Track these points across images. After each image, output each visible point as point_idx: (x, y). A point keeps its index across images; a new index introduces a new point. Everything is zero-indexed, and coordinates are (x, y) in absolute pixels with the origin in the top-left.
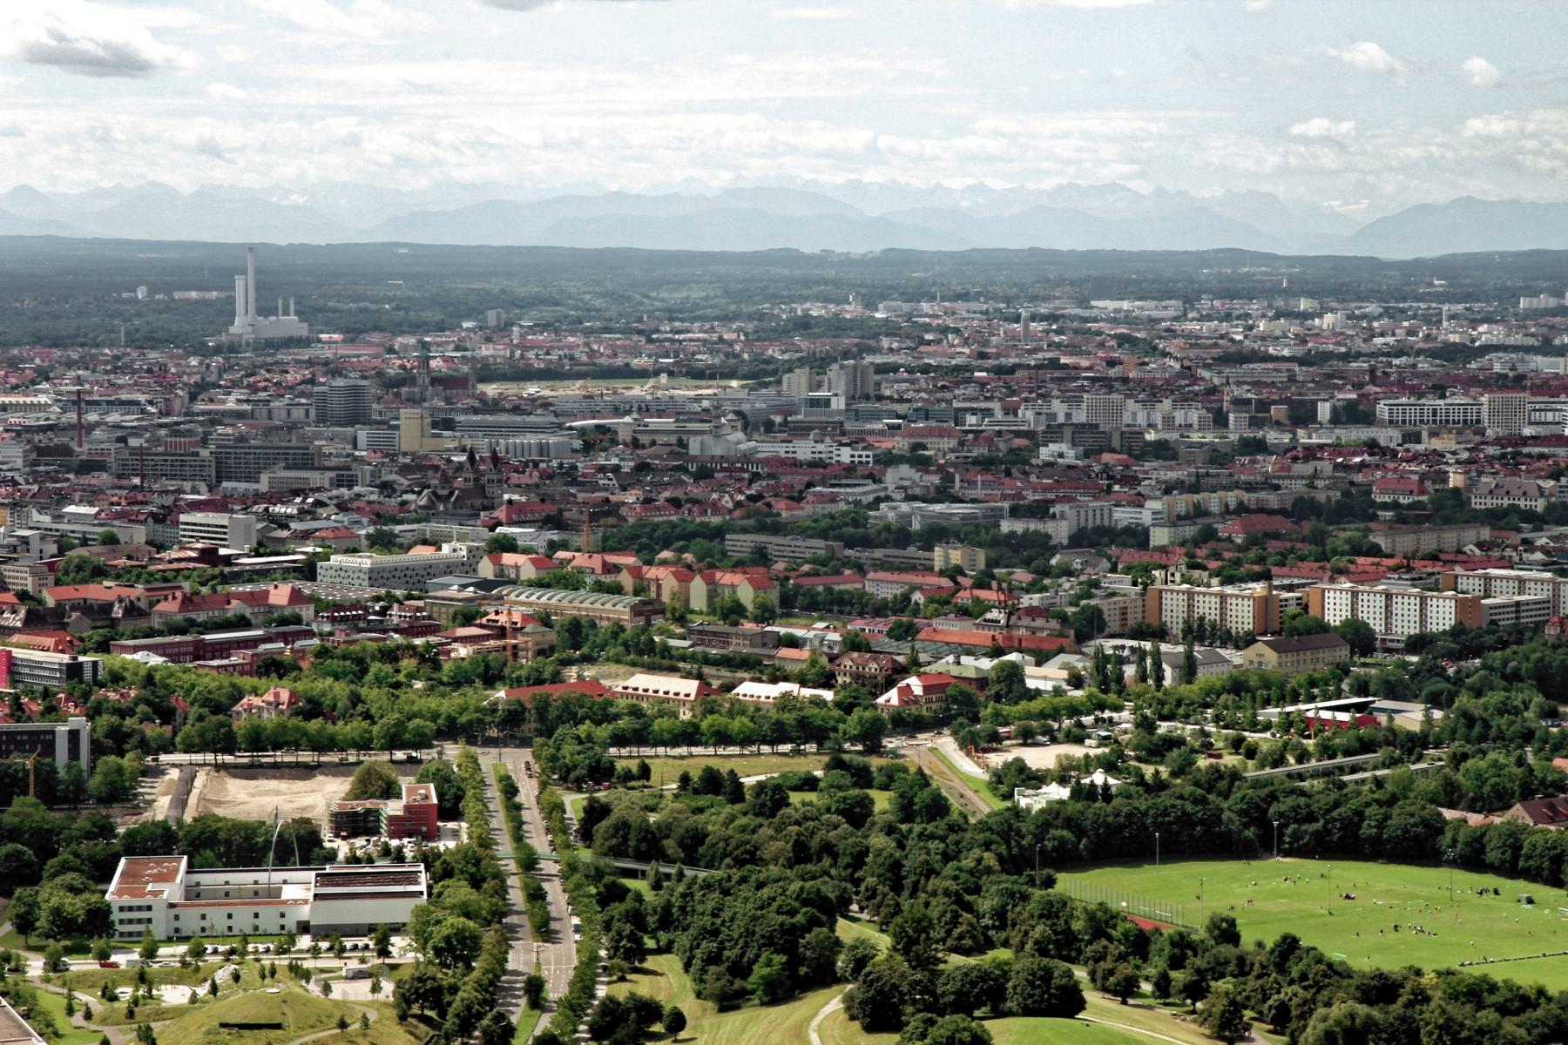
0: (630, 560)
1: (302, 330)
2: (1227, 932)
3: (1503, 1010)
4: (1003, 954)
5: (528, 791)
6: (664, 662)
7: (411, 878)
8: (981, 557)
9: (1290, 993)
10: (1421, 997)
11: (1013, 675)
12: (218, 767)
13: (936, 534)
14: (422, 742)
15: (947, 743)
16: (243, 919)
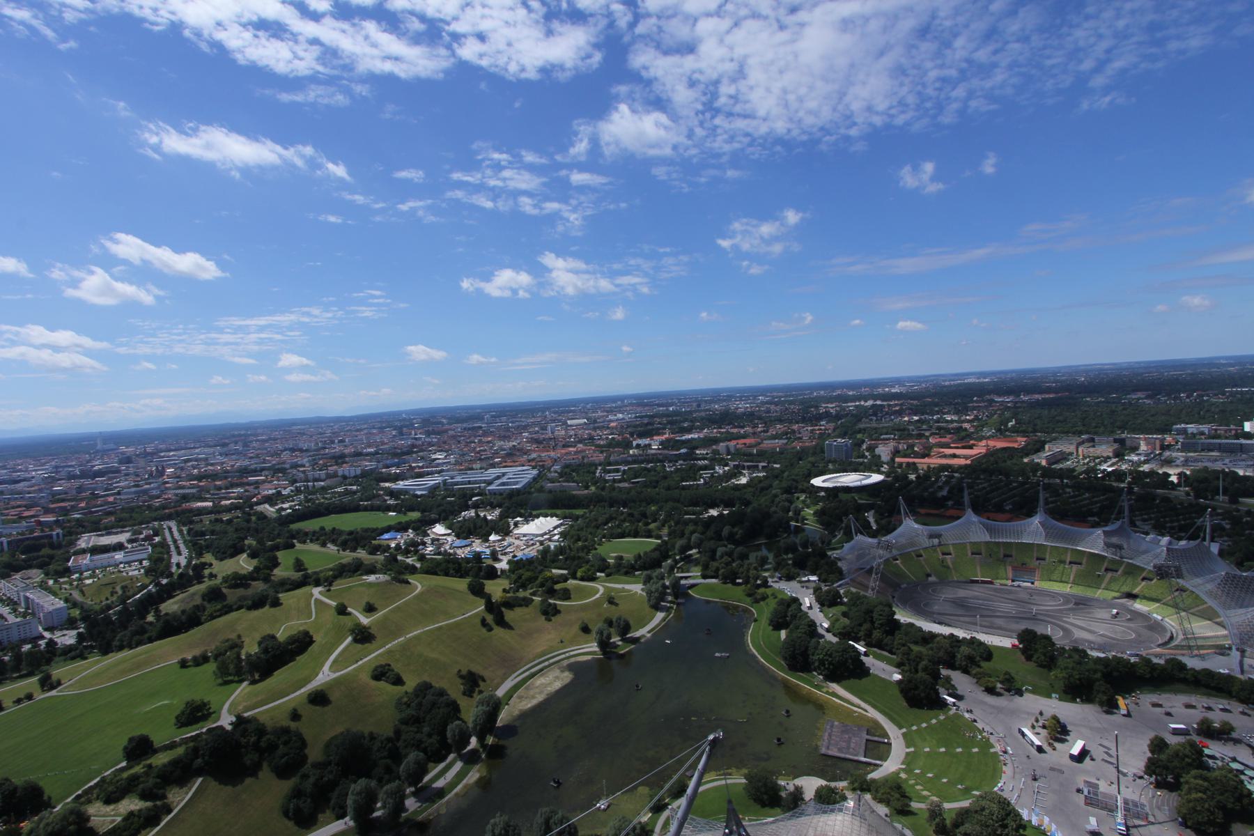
0: (195, 482)
1: (115, 447)
2: (322, 529)
3: (372, 532)
4: (278, 540)
5: (175, 529)
6: (205, 500)
7: (147, 549)
8: (272, 472)
9: (334, 537)
10: (357, 533)
11: (279, 493)
12: (97, 535)
13: (263, 469)
14: (148, 522)
15: (267, 506)
16: (105, 563)
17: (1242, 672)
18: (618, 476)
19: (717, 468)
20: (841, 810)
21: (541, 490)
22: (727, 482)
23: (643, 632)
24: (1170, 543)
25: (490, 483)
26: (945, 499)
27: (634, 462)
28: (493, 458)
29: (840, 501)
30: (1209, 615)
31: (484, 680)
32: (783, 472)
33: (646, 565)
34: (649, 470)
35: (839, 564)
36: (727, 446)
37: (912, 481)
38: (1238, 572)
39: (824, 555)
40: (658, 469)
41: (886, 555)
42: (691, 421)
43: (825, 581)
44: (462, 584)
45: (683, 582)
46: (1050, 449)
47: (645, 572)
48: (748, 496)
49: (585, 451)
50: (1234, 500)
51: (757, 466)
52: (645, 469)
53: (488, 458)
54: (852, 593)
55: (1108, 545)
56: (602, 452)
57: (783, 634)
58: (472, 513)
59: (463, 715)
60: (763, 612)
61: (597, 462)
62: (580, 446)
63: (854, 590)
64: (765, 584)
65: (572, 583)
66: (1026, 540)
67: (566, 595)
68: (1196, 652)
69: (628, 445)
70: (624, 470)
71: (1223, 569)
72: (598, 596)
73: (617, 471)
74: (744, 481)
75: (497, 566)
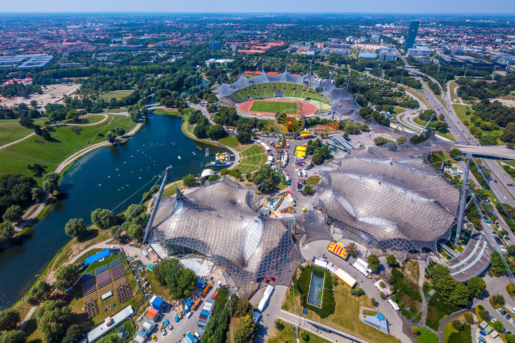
17: (333, 118)
18: (105, 59)
19: (159, 54)
20: (218, 182)
21: (58, 67)
22: (165, 61)
23: (132, 132)
24: (321, 80)
25: (20, 63)
26: (256, 67)
27: (113, 51)
28: (18, 48)
29: (216, 69)
30: (327, 103)
31: (47, 168)
32: (191, 56)
33: (130, 102)
34: (123, 55)
35: (216, 96)
36: (164, 43)
37: (244, 60)
38: (336, 88)
39: (210, 92)
40: (129, 55)
41: (234, 91)
42: (143, 29)
43: (211, 103)
44: (16, 123)
45: (149, 109)
46: (293, 46)
47: (129, 106)
48: (176, 67)
49: (82, 44)
50: (339, 66)
51: (179, 53)
52: (121, 54)
53: (14, 48)
54: (221, 106)
55: (305, 82)
56: (93, 45)
57: (195, 125)
58: (11, 82)
59: (38, 185)
60: (186, 118)
61: (91, 51)
62: (79, 42)
63: (222, 105)
64: (187, 106)
65: (88, 115)
66: (281, 81)
67: (86, 121)
68: (323, 114)
69: (108, 42)
70: (109, 56)
71: (334, 88)
72: (105, 119)
73: (105, 56)
74: (173, 60)
75: (39, 110)
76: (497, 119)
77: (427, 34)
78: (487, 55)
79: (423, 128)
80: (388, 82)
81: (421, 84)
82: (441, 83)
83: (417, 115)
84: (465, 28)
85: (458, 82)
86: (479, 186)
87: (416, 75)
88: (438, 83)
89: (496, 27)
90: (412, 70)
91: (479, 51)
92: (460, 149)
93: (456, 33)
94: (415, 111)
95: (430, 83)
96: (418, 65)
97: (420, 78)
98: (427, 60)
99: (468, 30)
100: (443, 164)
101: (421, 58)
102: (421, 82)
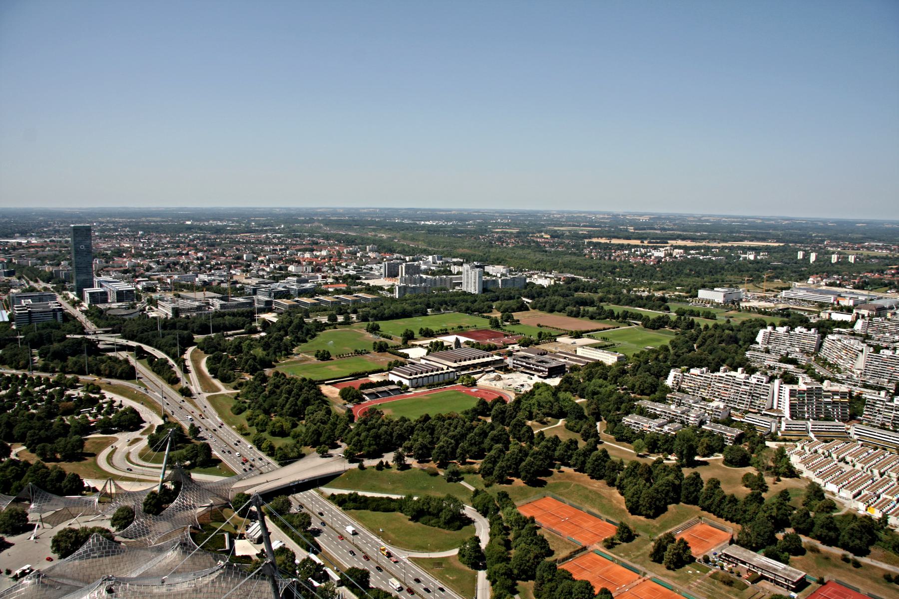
76: (287, 406)
77: (119, 253)
78: (238, 286)
79: (160, 468)
80: (53, 378)
81: (133, 368)
82: (174, 357)
83: (145, 442)
84: (188, 236)
85: (206, 347)
86: (301, 555)
87: (115, 347)
88: (169, 359)
89: (237, 233)
90: (106, 340)
91: (223, 279)
92: (247, 492)
93: (174, 247)
94: (136, 434)
95: (151, 360)
96: (114, 325)
97: (123, 355)
98: (131, 311)
99: (193, 240)
100: (226, 535)
101: (119, 308)
102: (133, 361)
